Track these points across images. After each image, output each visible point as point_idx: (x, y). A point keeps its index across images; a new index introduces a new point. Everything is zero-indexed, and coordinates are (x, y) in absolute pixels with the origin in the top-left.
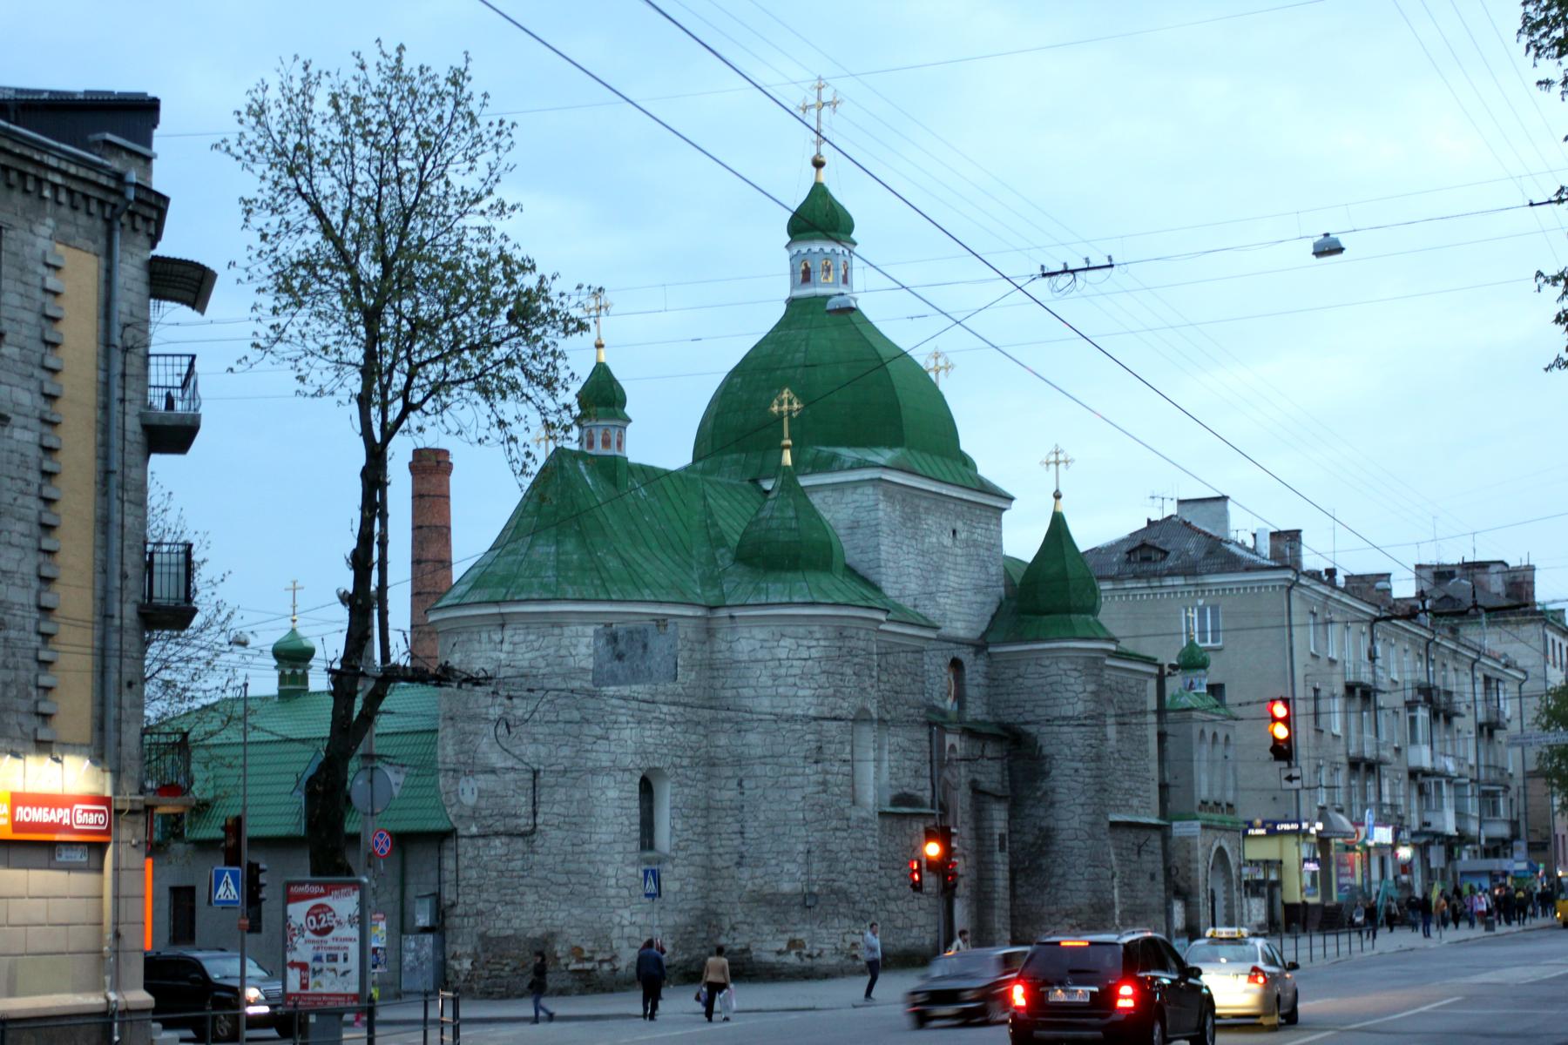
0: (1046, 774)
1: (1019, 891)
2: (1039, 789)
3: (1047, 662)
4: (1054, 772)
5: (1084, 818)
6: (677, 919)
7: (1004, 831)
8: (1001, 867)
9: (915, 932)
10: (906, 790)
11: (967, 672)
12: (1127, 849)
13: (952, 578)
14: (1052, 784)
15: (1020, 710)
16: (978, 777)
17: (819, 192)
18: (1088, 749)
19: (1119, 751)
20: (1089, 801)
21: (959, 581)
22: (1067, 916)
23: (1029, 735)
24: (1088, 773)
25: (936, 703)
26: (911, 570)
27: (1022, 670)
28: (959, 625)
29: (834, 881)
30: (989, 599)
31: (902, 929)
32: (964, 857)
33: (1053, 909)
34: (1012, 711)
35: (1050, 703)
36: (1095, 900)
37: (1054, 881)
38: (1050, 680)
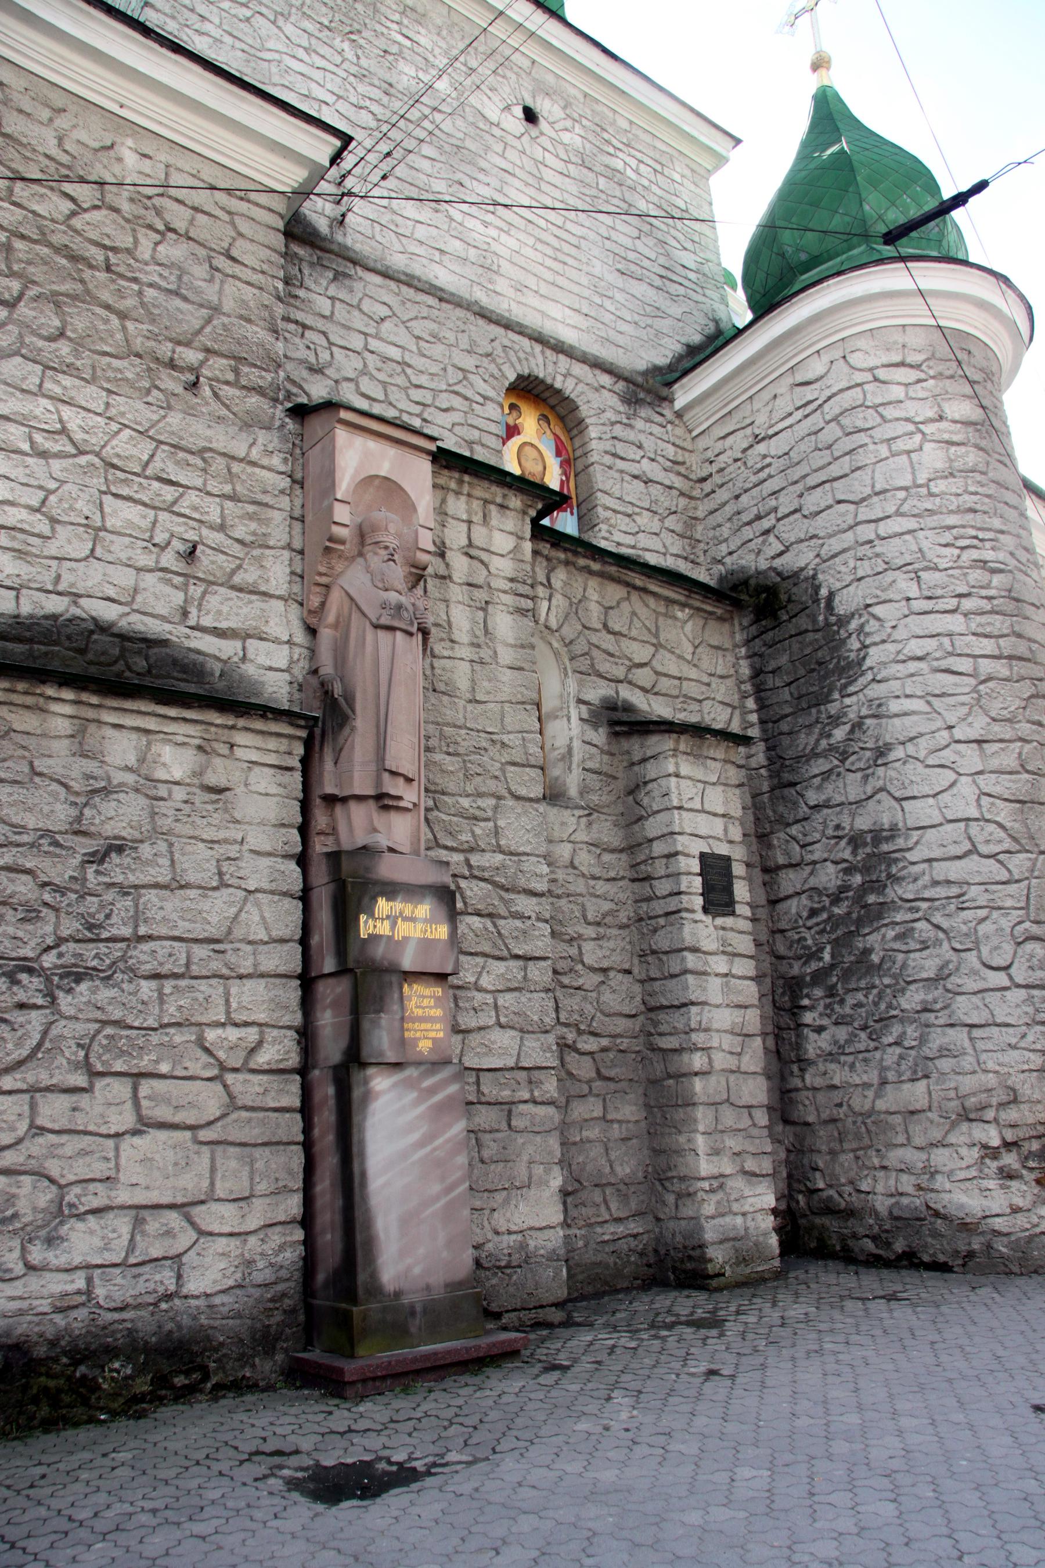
0: (852, 669)
1: (815, 1044)
2: (836, 720)
3: (817, 368)
4: (874, 657)
5: (987, 783)
7: (722, 849)
8: (720, 964)
10: (108, 613)
11: (593, 432)
14: (876, 691)
15: (766, 524)
16: (626, 693)
18: (976, 576)
20: (999, 730)
22: (967, 1116)
23: (794, 577)
24: (988, 646)
27: (761, 419)
28: (555, 311)
30: (676, 310)
33: (917, 1093)
34: (748, 533)
35: (835, 470)
37: (912, 999)
38: (832, 409)
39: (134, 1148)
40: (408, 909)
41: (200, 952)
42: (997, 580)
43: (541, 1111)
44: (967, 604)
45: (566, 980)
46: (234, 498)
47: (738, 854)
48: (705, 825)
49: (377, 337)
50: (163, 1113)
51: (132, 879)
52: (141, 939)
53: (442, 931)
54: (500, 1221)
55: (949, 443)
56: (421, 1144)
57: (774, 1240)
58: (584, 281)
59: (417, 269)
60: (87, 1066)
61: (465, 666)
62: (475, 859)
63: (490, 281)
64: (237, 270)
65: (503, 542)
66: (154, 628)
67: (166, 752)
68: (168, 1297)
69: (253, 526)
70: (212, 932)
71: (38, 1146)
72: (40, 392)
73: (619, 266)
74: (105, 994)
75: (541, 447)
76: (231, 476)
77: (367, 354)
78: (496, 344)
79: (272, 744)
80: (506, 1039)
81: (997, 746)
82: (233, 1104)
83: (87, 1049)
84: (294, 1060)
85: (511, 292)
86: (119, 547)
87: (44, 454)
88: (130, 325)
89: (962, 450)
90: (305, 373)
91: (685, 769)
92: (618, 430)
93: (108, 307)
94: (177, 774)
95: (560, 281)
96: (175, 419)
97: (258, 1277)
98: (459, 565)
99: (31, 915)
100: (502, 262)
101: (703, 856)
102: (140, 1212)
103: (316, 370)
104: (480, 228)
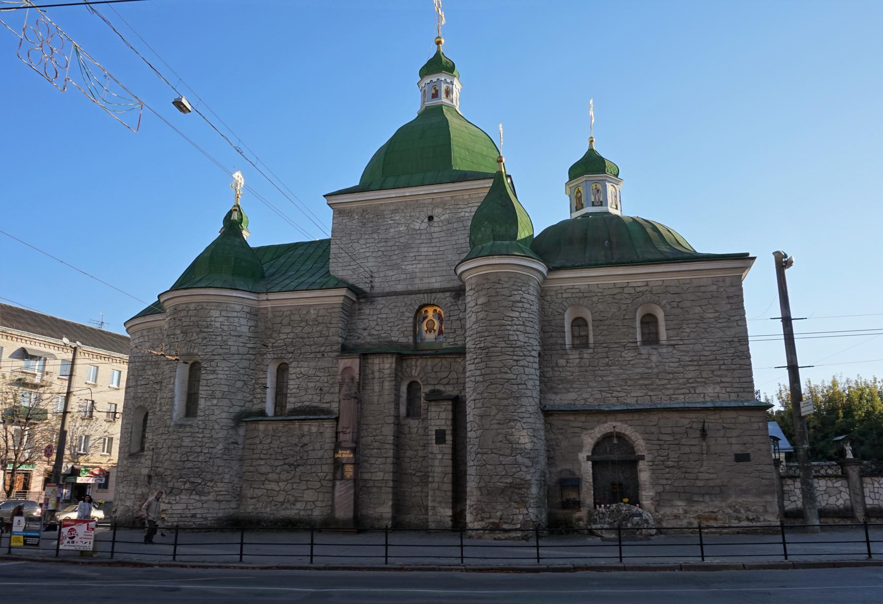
6: (144, 491)
7: (444, 428)
9: (299, 505)
10: (307, 404)
12: (673, 434)
13: (426, 249)
16: (437, 387)
17: (438, 55)
19: (673, 345)
21: (436, 249)
24: (478, 372)
25: (393, 339)
26: (368, 254)
28: (433, 280)
29: (157, 467)
31: (282, 503)
32: (354, 450)
36: (482, 484)
39: (307, 492)
40: (345, 452)
41: (317, 461)
42: (484, 351)
43: (387, 489)
44: (476, 361)
45: (413, 460)
46: (329, 376)
47: (451, 428)
48: (438, 422)
49: (380, 314)
50: (310, 487)
51: (308, 449)
52: (307, 459)
53: (351, 456)
54: (377, 510)
55: (477, 312)
56: (345, 493)
57: (450, 523)
58: (445, 265)
59: (392, 290)
60: (300, 479)
61: (376, 397)
62: (376, 438)
63: (413, 281)
64: (332, 326)
65: (387, 366)
66: (315, 404)
67: (313, 428)
68: (311, 515)
69: (333, 380)
70: (319, 457)
71: (293, 491)
72: (298, 367)
73: (458, 252)
74: (302, 468)
75: (434, 320)
76: (329, 372)
77: (378, 320)
78: (413, 301)
79: (330, 423)
80: (381, 474)
81: (478, 401)
82: (322, 485)
83: (300, 476)
84: (332, 478)
85: (419, 282)
86: (310, 391)
87: (299, 378)
88: (312, 347)
89: (480, 313)
90: (363, 331)
91: (433, 409)
92: (452, 308)
93: (308, 345)
94: (314, 431)
95: (436, 269)
96: (319, 363)
97: (324, 514)
98: (377, 374)
99: (293, 456)
100: (417, 274)
101: (436, 430)
102: (307, 502)
103: (365, 329)
104: (411, 267)
